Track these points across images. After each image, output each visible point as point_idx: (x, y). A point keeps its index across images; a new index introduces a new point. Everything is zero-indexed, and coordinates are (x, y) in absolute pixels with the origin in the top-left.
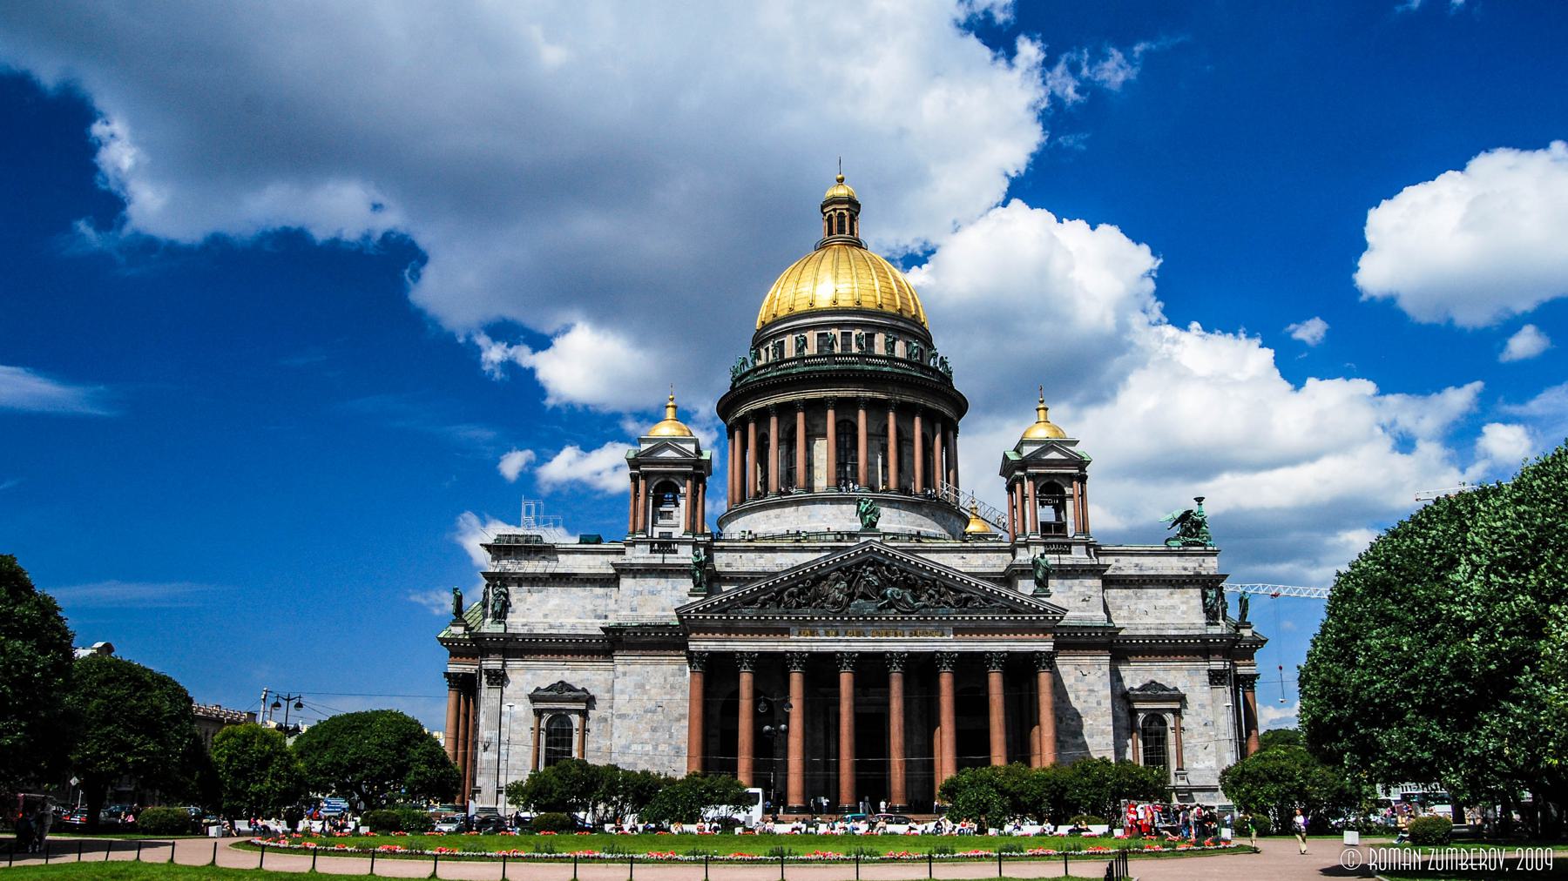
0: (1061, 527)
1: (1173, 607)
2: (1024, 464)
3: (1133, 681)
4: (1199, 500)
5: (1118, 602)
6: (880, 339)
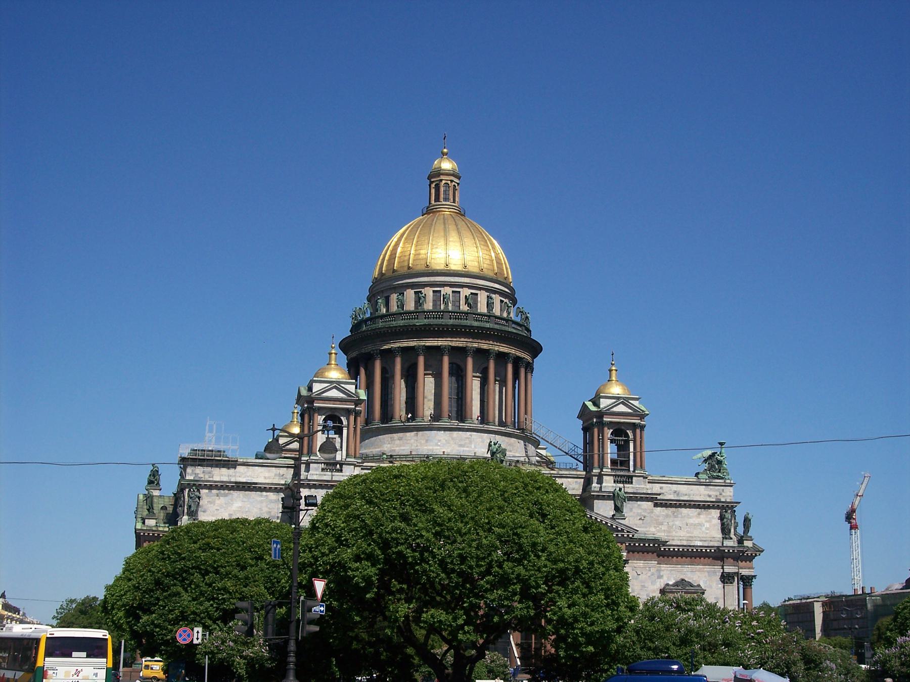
0: (625, 463)
1: (700, 525)
2: (600, 415)
3: (669, 579)
4: (721, 444)
5: (661, 519)
6: (482, 297)
